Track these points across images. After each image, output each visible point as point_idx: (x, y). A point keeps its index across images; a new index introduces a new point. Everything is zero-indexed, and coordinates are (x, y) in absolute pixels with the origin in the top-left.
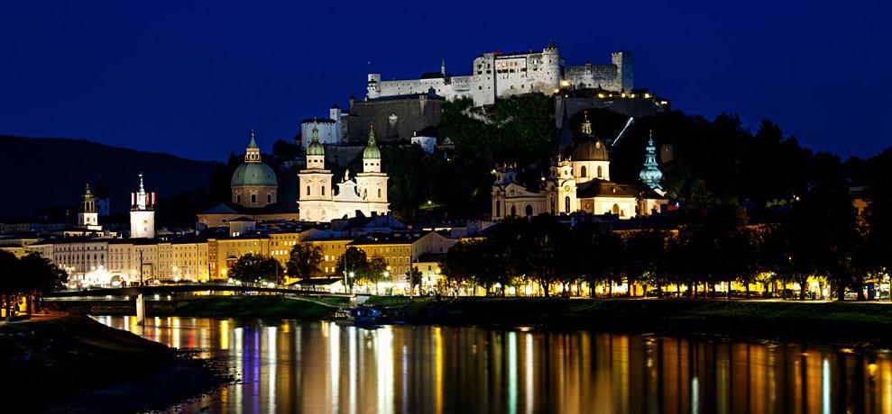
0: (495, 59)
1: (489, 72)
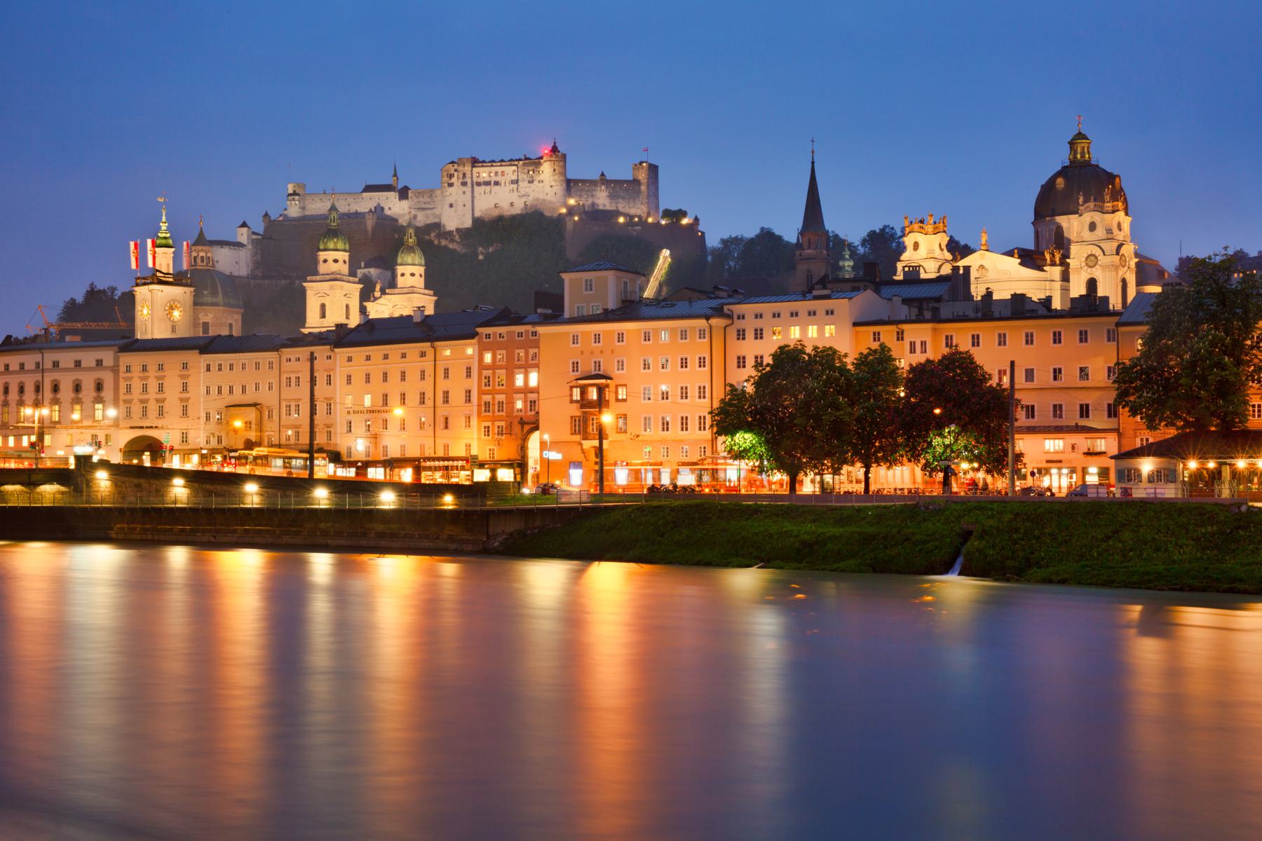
0: (473, 166)
1: (464, 184)
